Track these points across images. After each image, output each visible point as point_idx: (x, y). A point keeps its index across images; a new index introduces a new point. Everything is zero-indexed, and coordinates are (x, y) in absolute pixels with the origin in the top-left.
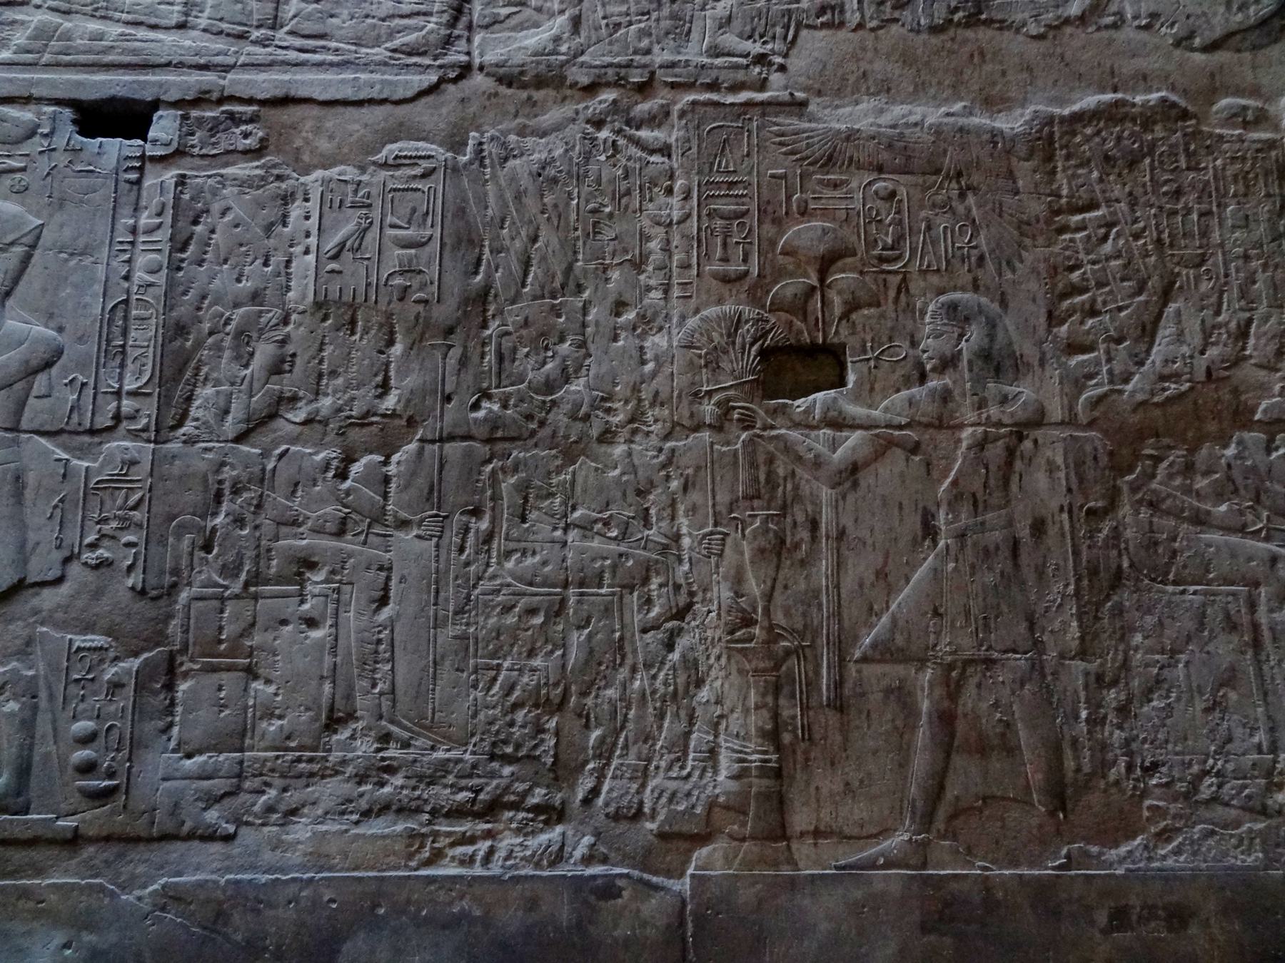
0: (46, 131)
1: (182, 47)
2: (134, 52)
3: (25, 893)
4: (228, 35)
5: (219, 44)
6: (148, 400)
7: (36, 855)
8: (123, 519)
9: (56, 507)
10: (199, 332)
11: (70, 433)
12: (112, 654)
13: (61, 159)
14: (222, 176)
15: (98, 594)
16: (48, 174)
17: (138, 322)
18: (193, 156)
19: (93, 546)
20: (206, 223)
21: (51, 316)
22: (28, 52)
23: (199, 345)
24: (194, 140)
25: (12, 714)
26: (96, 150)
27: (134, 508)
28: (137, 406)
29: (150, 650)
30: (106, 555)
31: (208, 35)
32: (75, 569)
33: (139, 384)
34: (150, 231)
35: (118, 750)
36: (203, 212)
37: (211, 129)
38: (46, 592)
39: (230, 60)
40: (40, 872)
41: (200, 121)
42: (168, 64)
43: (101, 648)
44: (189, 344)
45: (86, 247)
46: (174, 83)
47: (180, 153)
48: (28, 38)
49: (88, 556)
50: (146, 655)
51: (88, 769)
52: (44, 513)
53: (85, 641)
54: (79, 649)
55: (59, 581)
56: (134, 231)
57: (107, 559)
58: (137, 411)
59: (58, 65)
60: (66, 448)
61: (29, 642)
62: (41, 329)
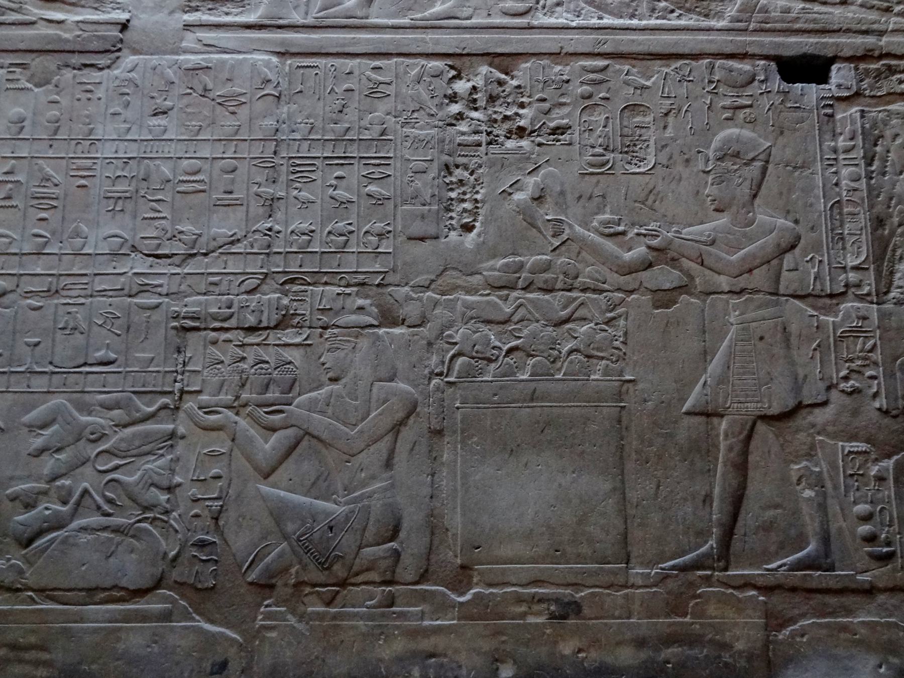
0: (762, 78)
1: (846, 18)
2: (814, 21)
3: (844, 628)
4: (878, 9)
5: (873, 16)
6: (866, 273)
7: (848, 600)
8: (865, 359)
9: (815, 350)
10: (892, 223)
11: (816, 296)
12: (873, 457)
13: (778, 99)
14: (888, 111)
15: (855, 413)
16: (769, 109)
17: (851, 217)
18: (865, 97)
19: (846, 378)
20: (882, 145)
21: (788, 212)
22: (738, 21)
23: (892, 234)
24: (865, 85)
25: (809, 499)
26: (800, 92)
27: (871, 351)
28: (861, 278)
29: (897, 454)
30: (857, 385)
31: (864, 10)
32: (834, 395)
33: (859, 262)
34: (847, 151)
35: (890, 526)
36: (879, 137)
37: (875, 77)
38: (817, 411)
39: (882, 27)
40: (849, 612)
41: (867, 72)
42: (839, 31)
43: (865, 452)
44: (886, 232)
45: (804, 162)
46: (847, 44)
47: (858, 94)
48: (739, 11)
49: (847, 386)
50: (896, 457)
51: (871, 539)
52: (807, 355)
53: (852, 447)
54: (850, 452)
55: (825, 404)
56: (835, 151)
57: (858, 388)
58: (861, 281)
59: (762, 30)
60: (814, 307)
61: (812, 447)
62: (782, 221)
